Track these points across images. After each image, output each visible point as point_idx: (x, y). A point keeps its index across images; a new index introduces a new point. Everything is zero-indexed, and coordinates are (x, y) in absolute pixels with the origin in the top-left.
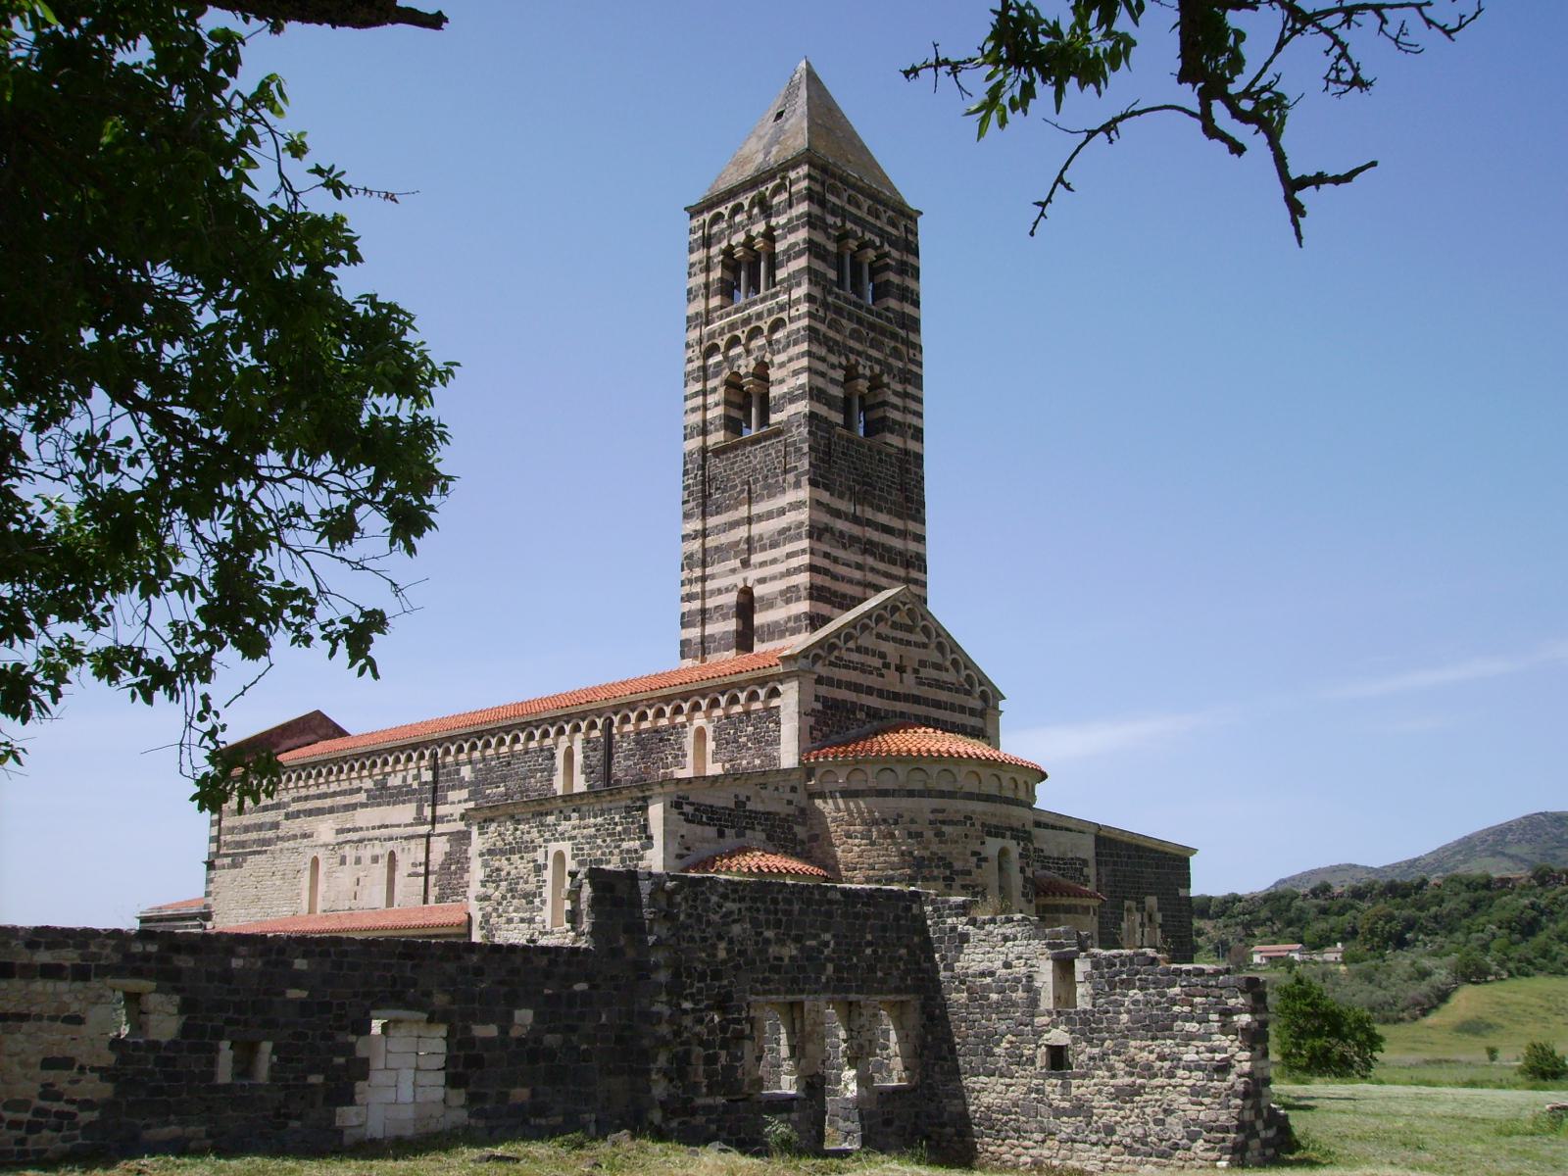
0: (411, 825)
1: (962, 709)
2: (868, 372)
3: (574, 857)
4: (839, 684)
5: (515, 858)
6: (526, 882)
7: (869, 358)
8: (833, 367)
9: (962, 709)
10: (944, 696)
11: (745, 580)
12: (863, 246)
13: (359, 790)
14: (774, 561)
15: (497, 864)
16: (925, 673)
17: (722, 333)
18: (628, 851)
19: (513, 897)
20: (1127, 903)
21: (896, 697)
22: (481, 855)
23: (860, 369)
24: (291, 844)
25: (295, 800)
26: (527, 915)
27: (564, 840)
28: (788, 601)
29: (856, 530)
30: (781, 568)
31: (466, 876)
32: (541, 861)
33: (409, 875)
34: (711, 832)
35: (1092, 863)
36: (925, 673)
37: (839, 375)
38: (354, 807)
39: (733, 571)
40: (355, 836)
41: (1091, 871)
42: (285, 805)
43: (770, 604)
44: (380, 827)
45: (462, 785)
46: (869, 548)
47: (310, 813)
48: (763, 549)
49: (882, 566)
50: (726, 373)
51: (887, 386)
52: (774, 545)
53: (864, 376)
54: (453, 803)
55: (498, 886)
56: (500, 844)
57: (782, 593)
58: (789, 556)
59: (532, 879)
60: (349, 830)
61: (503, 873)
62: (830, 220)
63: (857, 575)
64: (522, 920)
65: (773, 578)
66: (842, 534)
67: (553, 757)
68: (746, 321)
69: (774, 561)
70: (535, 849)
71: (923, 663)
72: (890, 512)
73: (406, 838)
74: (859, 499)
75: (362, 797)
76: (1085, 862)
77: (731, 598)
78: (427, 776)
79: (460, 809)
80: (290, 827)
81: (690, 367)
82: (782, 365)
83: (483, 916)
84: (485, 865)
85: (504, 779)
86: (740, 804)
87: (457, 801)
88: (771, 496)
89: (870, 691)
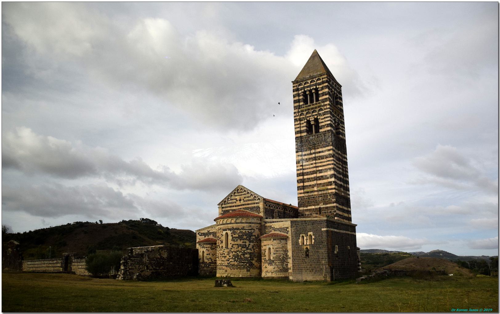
1: (254, 203)
4: (227, 207)
7: (314, 115)
9: (254, 203)
10: (250, 202)
12: (310, 91)
16: (245, 199)
20: (301, 235)
21: (239, 206)
29: (310, 156)
34: (203, 237)
35: (290, 227)
36: (245, 199)
37: (305, 124)
41: (289, 229)
46: (315, 159)
49: (319, 161)
62: (300, 92)
63: (312, 166)
66: (306, 159)
71: (245, 198)
72: (321, 148)
74: (310, 149)
76: (288, 228)
86: (208, 231)
89: (233, 206)
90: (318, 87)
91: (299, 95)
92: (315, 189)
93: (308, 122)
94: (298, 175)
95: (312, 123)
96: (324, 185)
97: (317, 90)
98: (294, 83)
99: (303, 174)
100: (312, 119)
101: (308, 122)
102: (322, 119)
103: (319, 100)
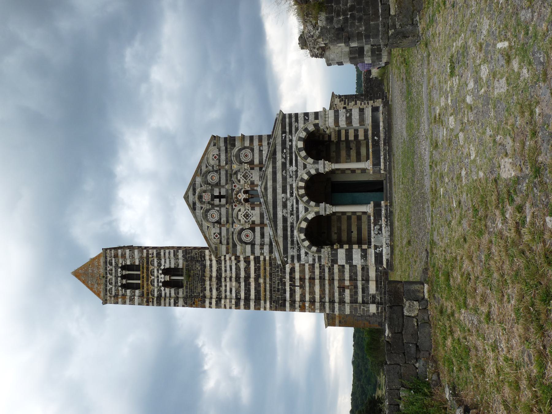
2: (163, 276)
8: (165, 294)
23: (163, 280)
37: (167, 290)
51: (164, 266)
53: (164, 278)
62: (120, 293)
90: (120, 265)
91: (124, 296)
92: (261, 281)
93: (166, 284)
94: (237, 306)
95: (167, 278)
96: (257, 269)
97: (124, 268)
98: (105, 302)
99: (238, 299)
100: (162, 278)
101: (166, 284)
102: (165, 262)
103: (139, 265)
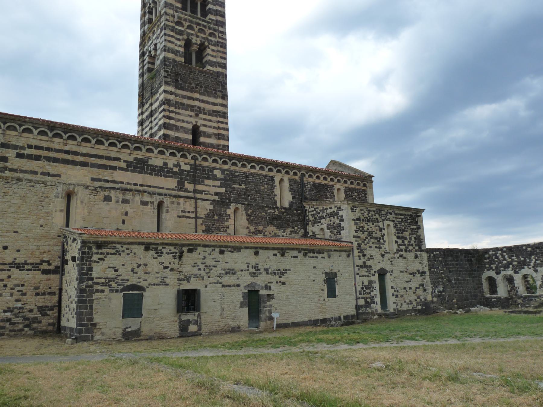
0: (173, 190)
3: (394, 227)
5: (370, 224)
6: (376, 233)
11: (196, 122)
13: (118, 159)
14: (210, 121)
15: (362, 225)
17: (185, 20)
18: (413, 229)
19: (371, 238)
22: (354, 220)
24: (29, 176)
25: (30, 147)
26: (378, 246)
27: (390, 221)
28: (219, 138)
30: (216, 125)
31: (226, 223)
32: (381, 226)
33: (179, 217)
38: (114, 168)
39: (191, 116)
40: (119, 186)
42: (15, 147)
43: (208, 136)
44: (141, 185)
45: (215, 178)
47: (56, 160)
48: (205, 114)
50: (185, 37)
52: (210, 115)
54: (208, 185)
55: (363, 233)
56: (362, 217)
57: (215, 134)
58: (219, 122)
59: (378, 232)
60: (108, 181)
61: (365, 229)
64: (376, 247)
65: (210, 127)
67: (272, 179)
68: (190, 21)
69: (210, 121)
70: (378, 222)
73: (175, 196)
75: (124, 165)
77: (190, 126)
78: (188, 168)
79: (213, 190)
80: (15, 162)
81: (167, 23)
82: (213, 50)
83: (358, 244)
84: (356, 224)
85: (244, 182)
87: (212, 187)
88: (208, 96)
